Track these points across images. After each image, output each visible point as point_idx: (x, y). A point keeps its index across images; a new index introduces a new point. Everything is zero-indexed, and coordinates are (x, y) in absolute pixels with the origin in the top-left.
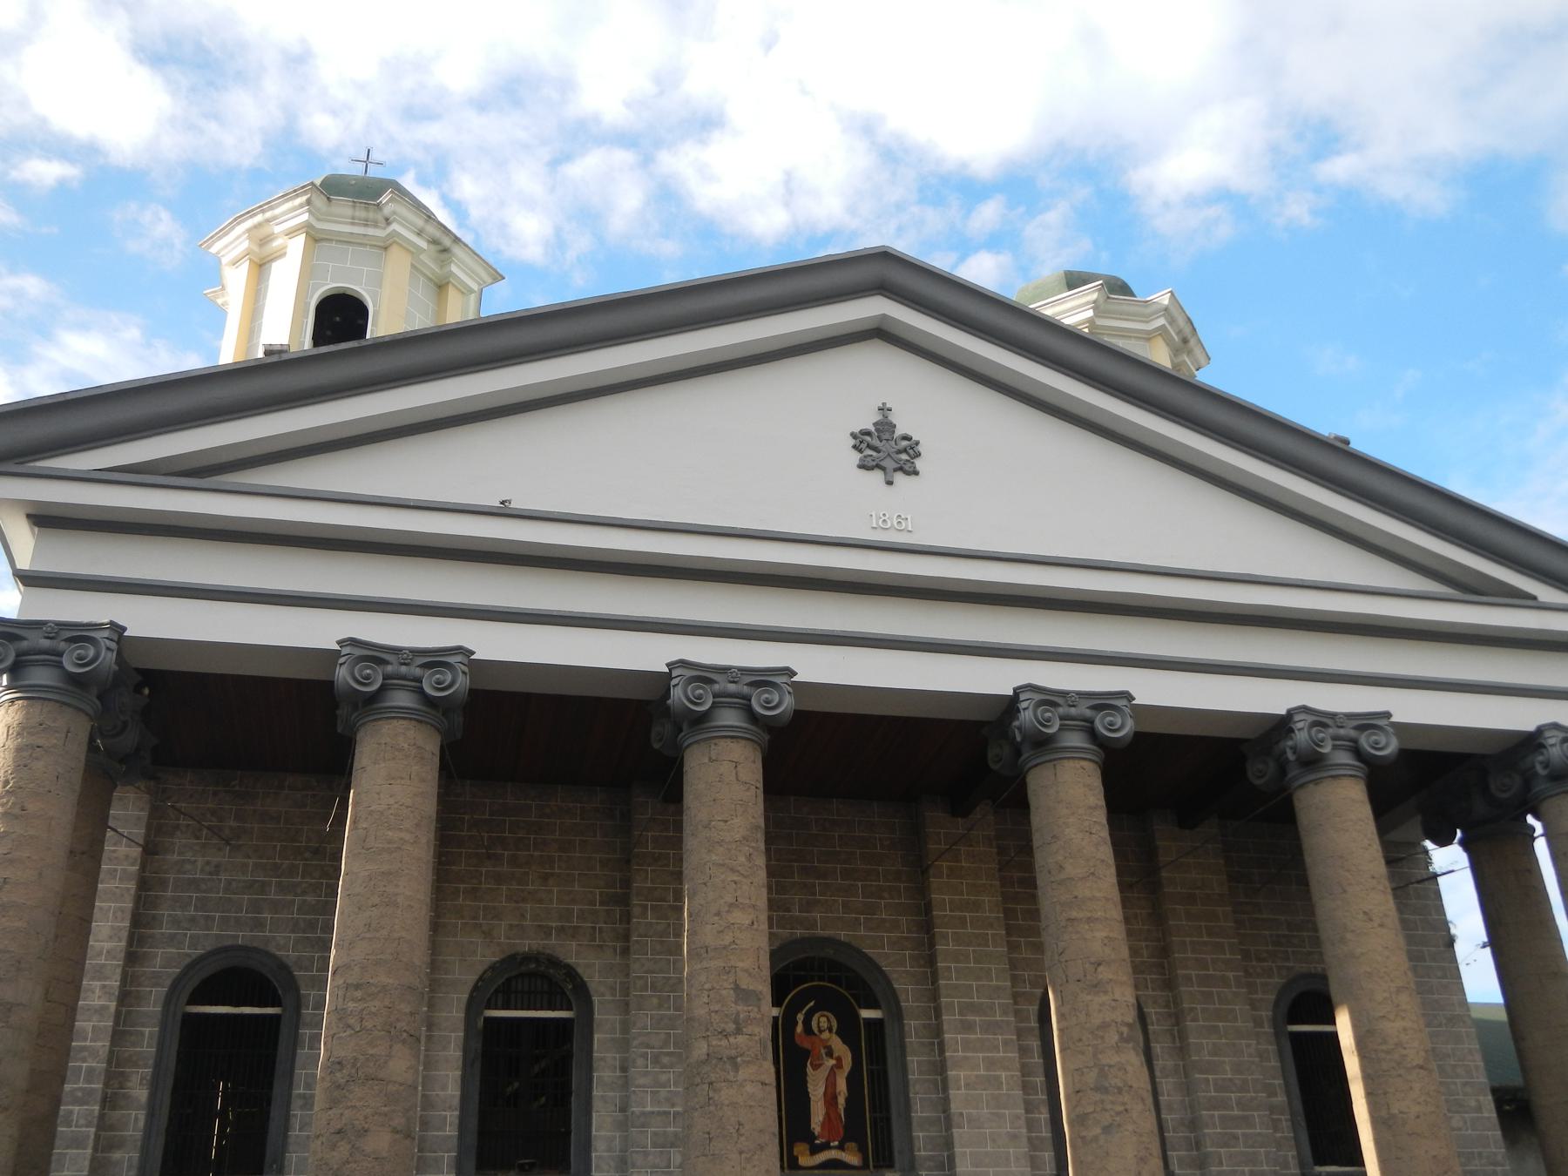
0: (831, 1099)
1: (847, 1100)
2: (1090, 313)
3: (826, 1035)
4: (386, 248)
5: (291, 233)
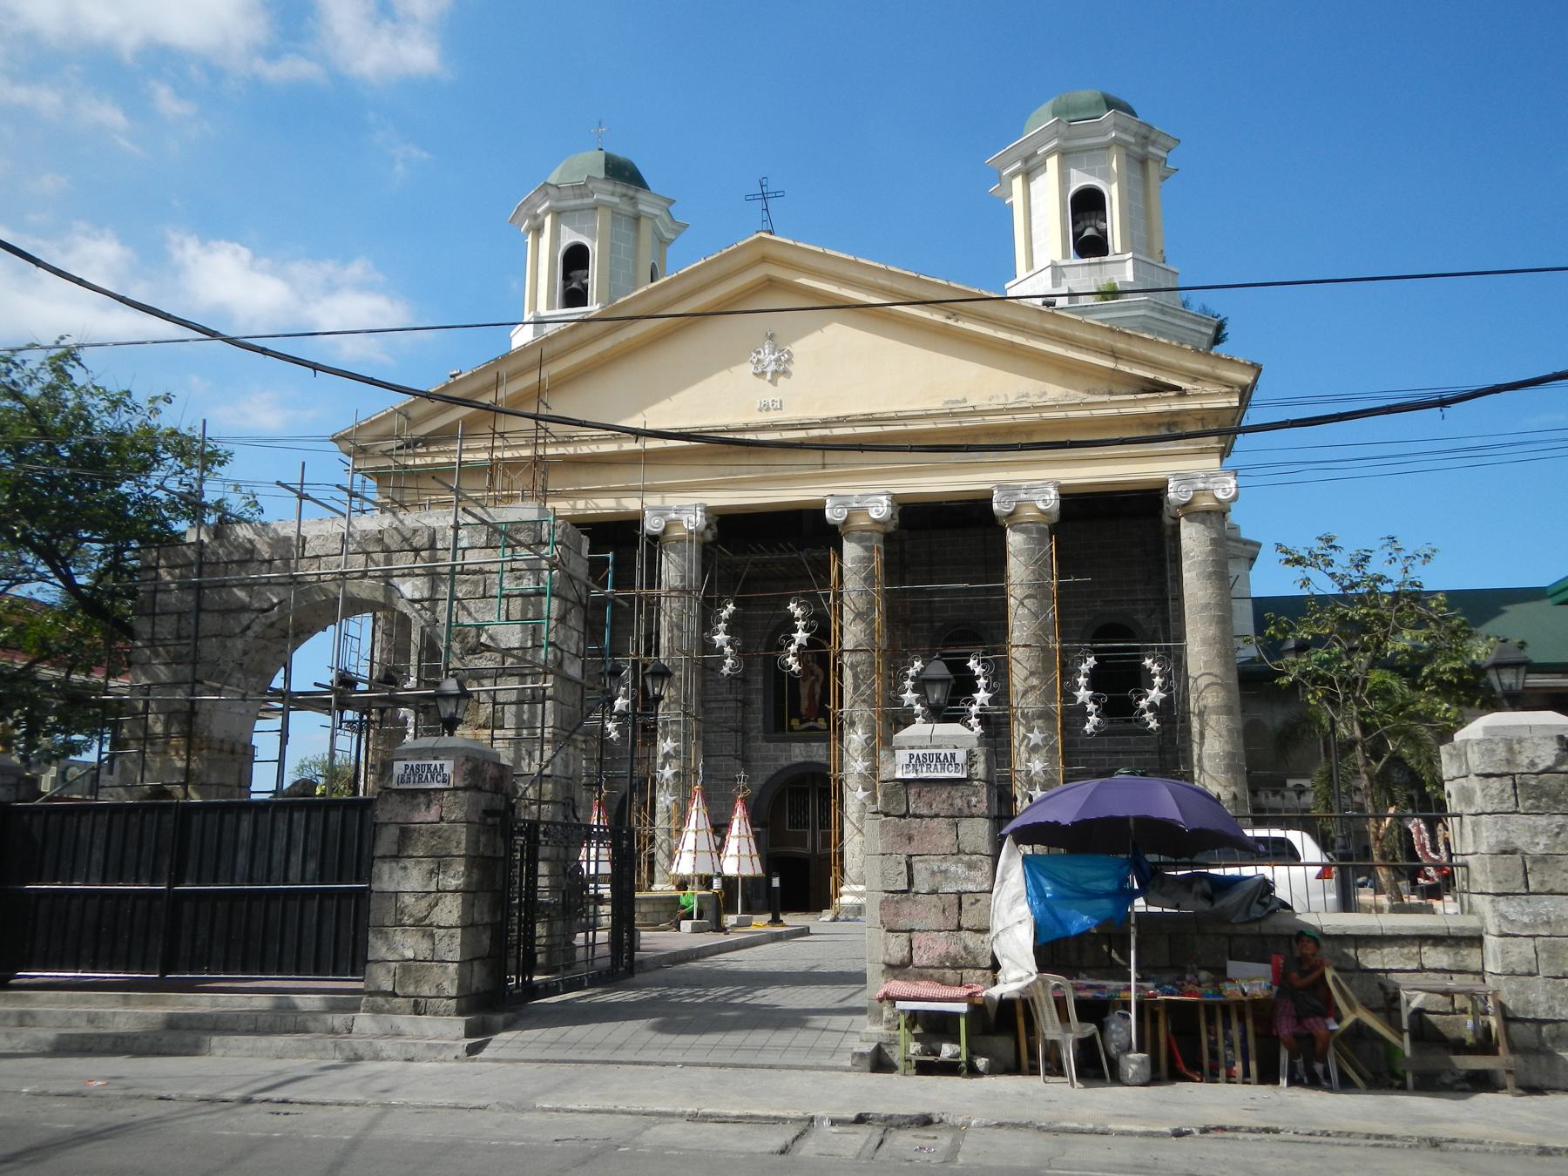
0: (811, 696)
1: (820, 697)
2: (1055, 143)
3: (811, 664)
4: (596, 208)
5: (546, 212)
